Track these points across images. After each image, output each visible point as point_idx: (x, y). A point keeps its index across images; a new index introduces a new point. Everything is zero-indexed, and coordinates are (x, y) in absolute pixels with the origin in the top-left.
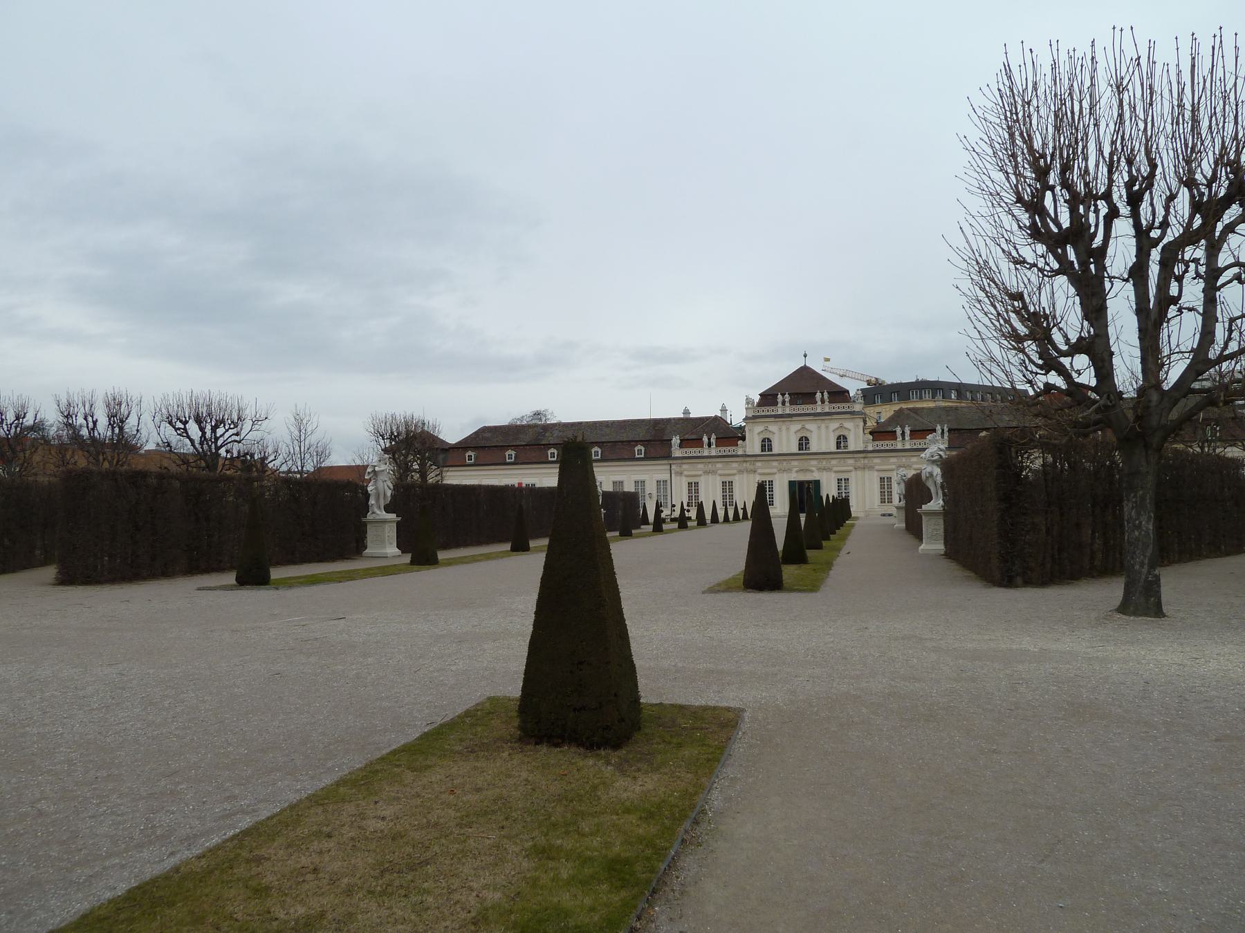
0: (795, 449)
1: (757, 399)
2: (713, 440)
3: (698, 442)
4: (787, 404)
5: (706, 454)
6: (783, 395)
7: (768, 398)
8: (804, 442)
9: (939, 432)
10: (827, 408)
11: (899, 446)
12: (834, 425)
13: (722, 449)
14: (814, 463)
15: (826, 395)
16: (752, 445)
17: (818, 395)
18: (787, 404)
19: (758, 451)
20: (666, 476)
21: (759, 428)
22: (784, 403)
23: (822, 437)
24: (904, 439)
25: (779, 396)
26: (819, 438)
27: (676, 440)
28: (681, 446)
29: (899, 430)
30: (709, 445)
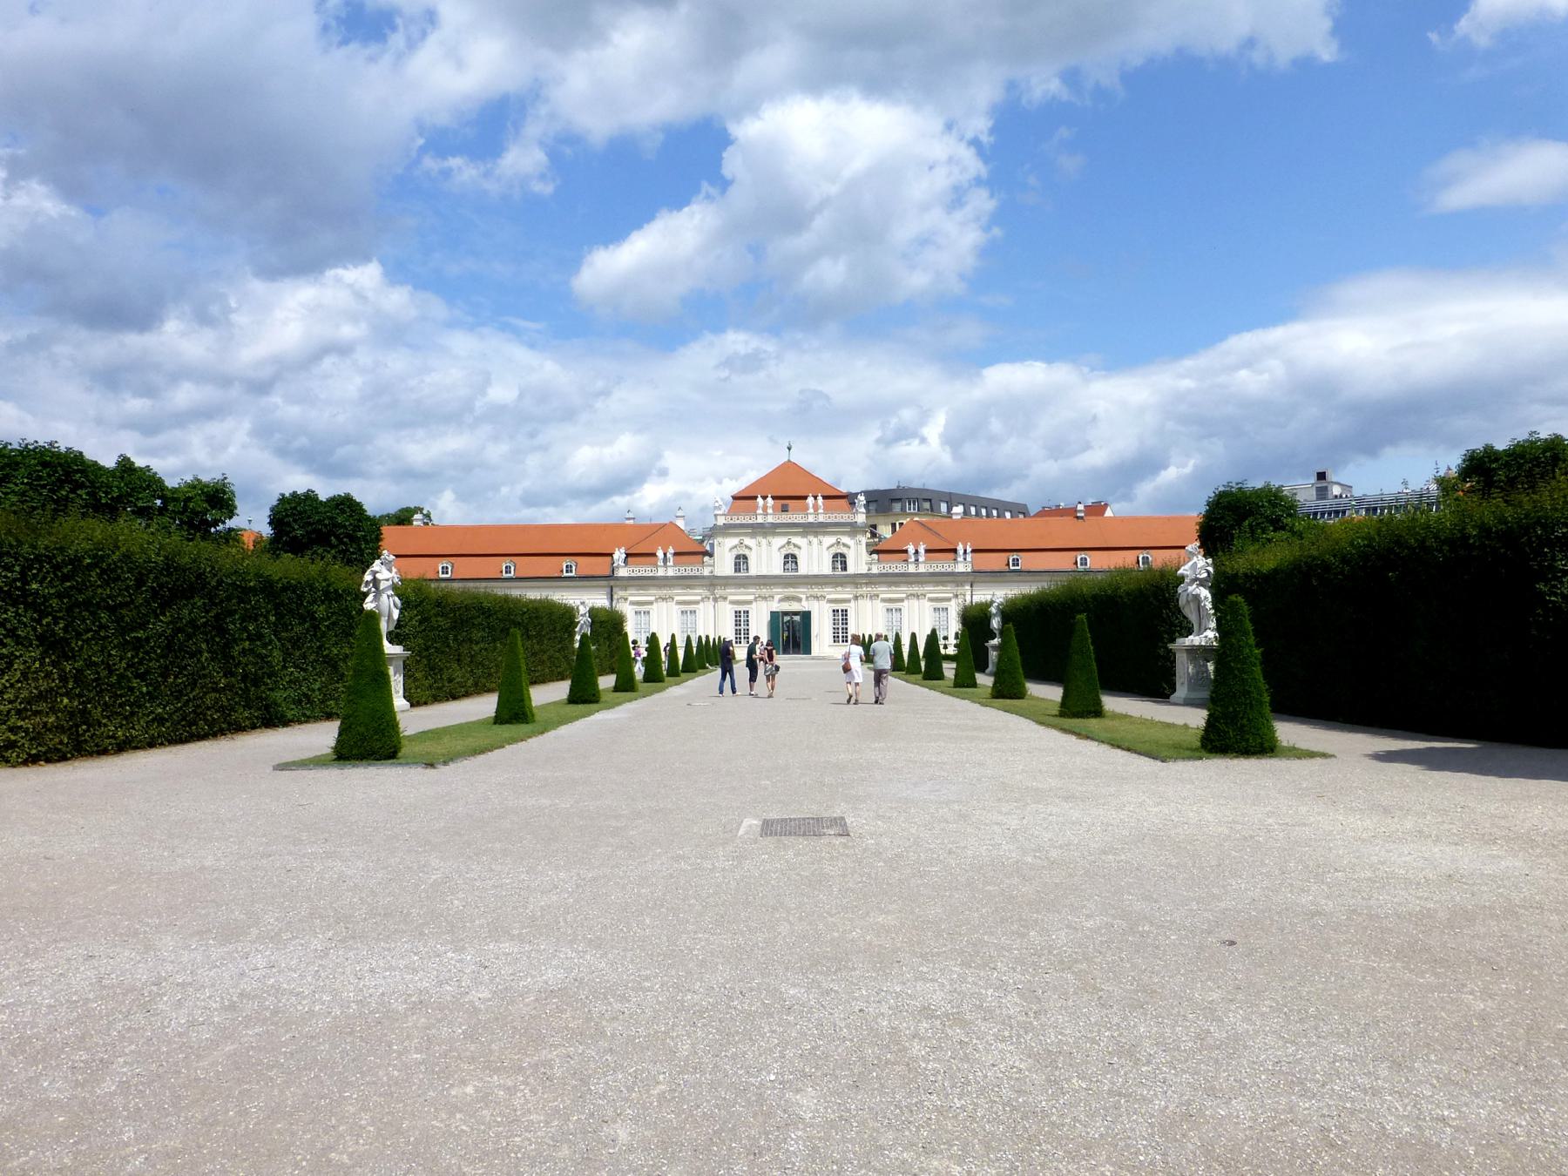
6: (764, 498)
7: (744, 498)
16: (723, 564)
21: (732, 541)
22: (765, 508)
25: (760, 500)
27: (619, 555)
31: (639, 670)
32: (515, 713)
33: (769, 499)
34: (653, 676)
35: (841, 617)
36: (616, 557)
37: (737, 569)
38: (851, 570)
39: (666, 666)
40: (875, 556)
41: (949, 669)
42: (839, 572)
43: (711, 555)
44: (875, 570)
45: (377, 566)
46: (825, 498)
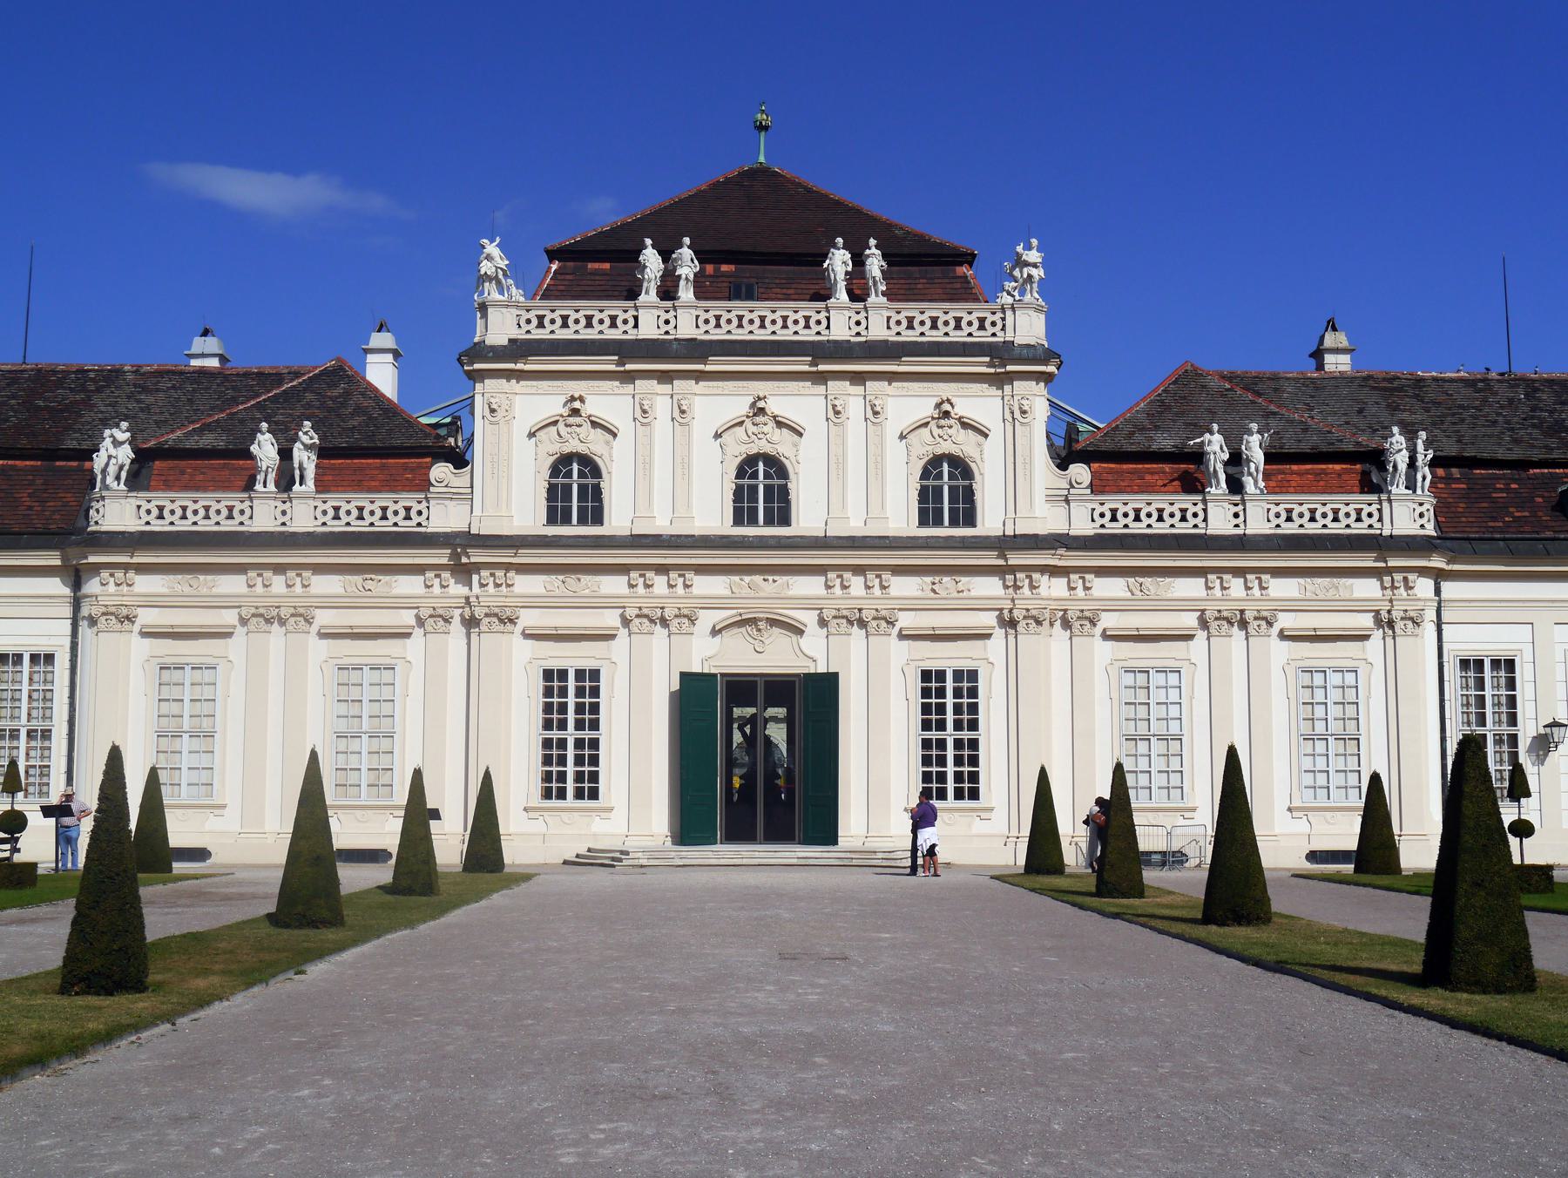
0: (711, 513)
3: (228, 464)
4: (686, 294)
8: (762, 487)
9: (1402, 460)
10: (881, 320)
11: (1220, 521)
12: (907, 404)
13: (350, 501)
14: (811, 586)
15: (875, 264)
17: (839, 261)
18: (686, 294)
20: (52, 633)
23: (855, 457)
24: (1235, 486)
25: (651, 259)
26: (835, 465)
27: (114, 452)
28: (137, 478)
29: (1215, 445)
30: (286, 480)
36: (99, 461)
38: (990, 521)
43: (460, 460)
44: (1083, 526)
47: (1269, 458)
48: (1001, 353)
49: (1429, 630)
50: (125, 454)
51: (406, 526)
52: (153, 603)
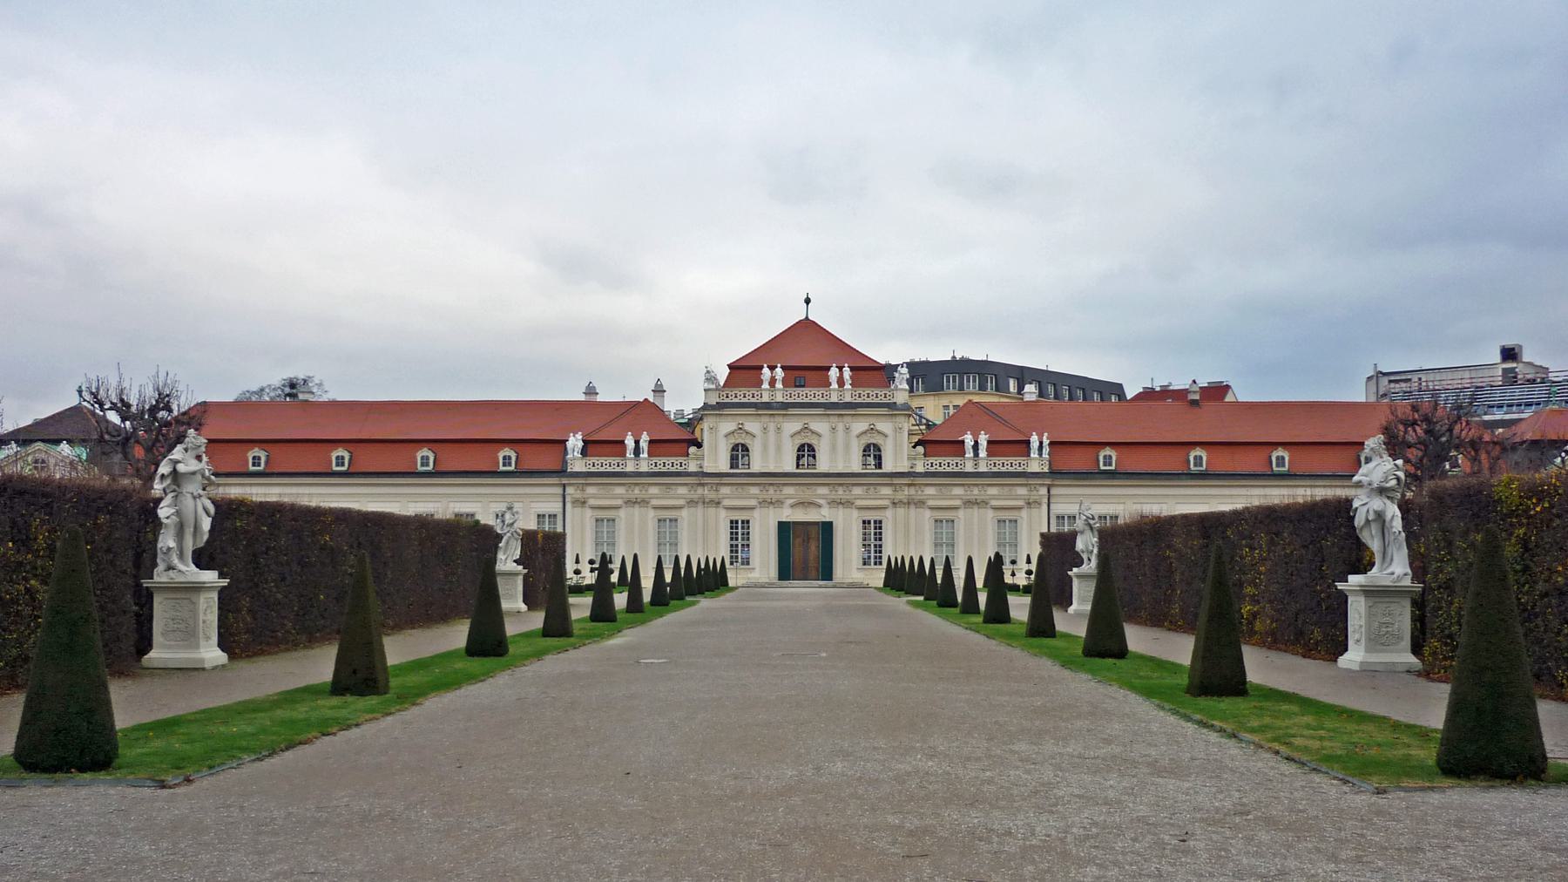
1: (722, 374)
2: (644, 445)
4: (779, 385)
5: (630, 468)
6: (772, 368)
7: (745, 371)
12: (860, 426)
16: (716, 457)
17: (834, 373)
18: (779, 385)
19: (723, 465)
21: (727, 426)
22: (773, 382)
25: (766, 371)
27: (575, 442)
28: (584, 452)
31: (580, 607)
32: (361, 677)
33: (779, 370)
34: (603, 613)
35: (873, 531)
36: (570, 444)
37: (734, 462)
38: (888, 467)
39: (618, 599)
40: (920, 449)
41: (1020, 608)
42: (872, 469)
43: (699, 445)
44: (920, 468)
45: (178, 453)
46: (852, 369)
47: (989, 442)
48: (892, 406)
49: (1045, 507)
50: (580, 444)
51: (680, 469)
52: (594, 497)
